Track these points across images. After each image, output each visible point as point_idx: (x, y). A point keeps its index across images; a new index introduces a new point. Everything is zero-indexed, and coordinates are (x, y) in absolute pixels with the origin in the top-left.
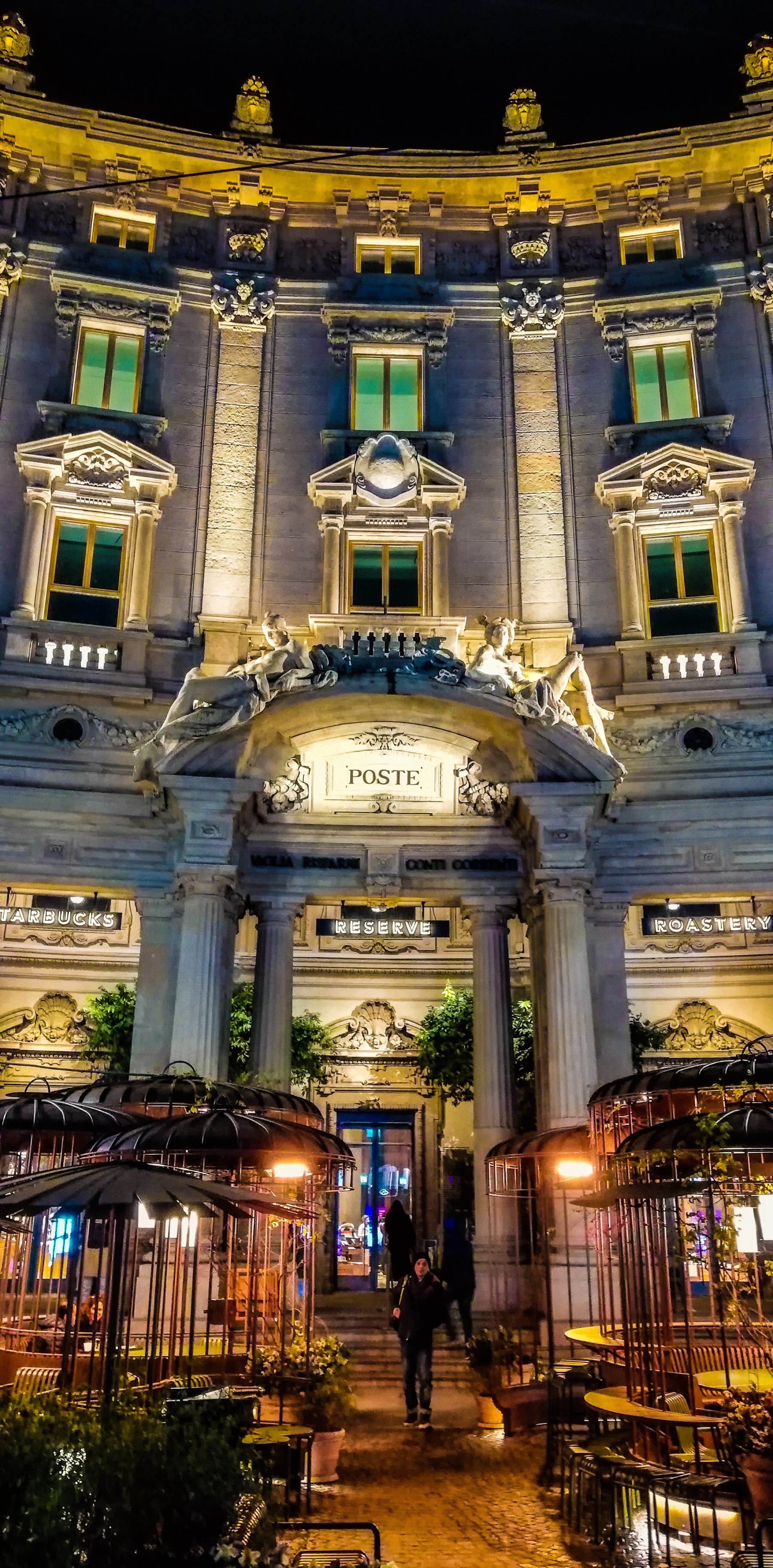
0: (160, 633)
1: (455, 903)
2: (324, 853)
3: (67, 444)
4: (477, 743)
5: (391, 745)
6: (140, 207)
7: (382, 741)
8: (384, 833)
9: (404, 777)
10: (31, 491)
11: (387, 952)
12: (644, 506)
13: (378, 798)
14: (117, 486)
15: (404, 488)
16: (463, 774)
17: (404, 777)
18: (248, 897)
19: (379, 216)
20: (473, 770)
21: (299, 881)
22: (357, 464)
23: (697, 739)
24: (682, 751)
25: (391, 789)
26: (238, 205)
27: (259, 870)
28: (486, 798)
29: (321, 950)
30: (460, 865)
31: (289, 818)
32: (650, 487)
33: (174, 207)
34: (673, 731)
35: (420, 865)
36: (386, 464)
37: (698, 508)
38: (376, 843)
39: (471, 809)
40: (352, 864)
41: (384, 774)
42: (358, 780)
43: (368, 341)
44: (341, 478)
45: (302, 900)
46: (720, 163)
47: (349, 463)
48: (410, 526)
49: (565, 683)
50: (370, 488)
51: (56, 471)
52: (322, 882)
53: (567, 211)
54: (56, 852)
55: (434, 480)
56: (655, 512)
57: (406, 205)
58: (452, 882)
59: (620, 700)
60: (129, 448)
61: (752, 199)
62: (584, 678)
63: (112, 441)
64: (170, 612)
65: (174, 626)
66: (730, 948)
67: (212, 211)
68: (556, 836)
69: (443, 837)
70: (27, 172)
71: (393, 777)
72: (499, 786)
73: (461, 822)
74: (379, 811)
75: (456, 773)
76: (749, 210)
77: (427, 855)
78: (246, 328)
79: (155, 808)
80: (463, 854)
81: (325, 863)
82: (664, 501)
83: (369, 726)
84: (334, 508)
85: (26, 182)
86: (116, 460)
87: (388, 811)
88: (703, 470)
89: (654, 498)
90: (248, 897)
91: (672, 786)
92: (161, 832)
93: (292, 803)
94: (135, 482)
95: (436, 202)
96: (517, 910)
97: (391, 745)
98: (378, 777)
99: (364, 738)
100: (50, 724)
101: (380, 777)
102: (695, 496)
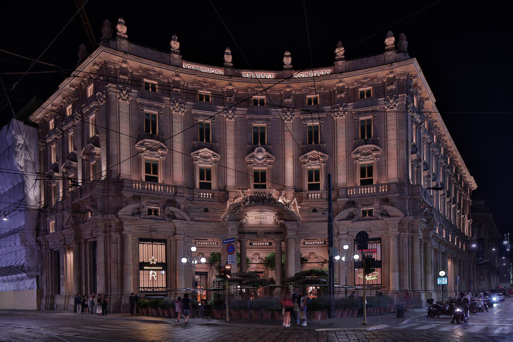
0: (220, 190)
1: (273, 239)
2: (251, 231)
6: (208, 90)
10: (194, 162)
13: (260, 222)
15: (263, 158)
21: (247, 236)
22: (254, 153)
25: (262, 220)
30: (273, 233)
31: (245, 226)
34: (310, 209)
36: (260, 153)
38: (259, 229)
40: (256, 233)
43: (255, 123)
47: (253, 153)
49: (293, 202)
50: (257, 158)
52: (251, 237)
53: (296, 90)
54: (207, 232)
55: (269, 157)
58: (272, 236)
59: (302, 203)
60: (211, 152)
61: (334, 91)
62: (296, 202)
64: (221, 185)
65: (222, 188)
67: (222, 90)
70: (184, 84)
73: (274, 226)
78: (231, 120)
83: (259, 209)
84: (251, 163)
86: (209, 154)
89: (310, 161)
91: (310, 219)
96: (283, 241)
101: (260, 218)
102: (318, 161)
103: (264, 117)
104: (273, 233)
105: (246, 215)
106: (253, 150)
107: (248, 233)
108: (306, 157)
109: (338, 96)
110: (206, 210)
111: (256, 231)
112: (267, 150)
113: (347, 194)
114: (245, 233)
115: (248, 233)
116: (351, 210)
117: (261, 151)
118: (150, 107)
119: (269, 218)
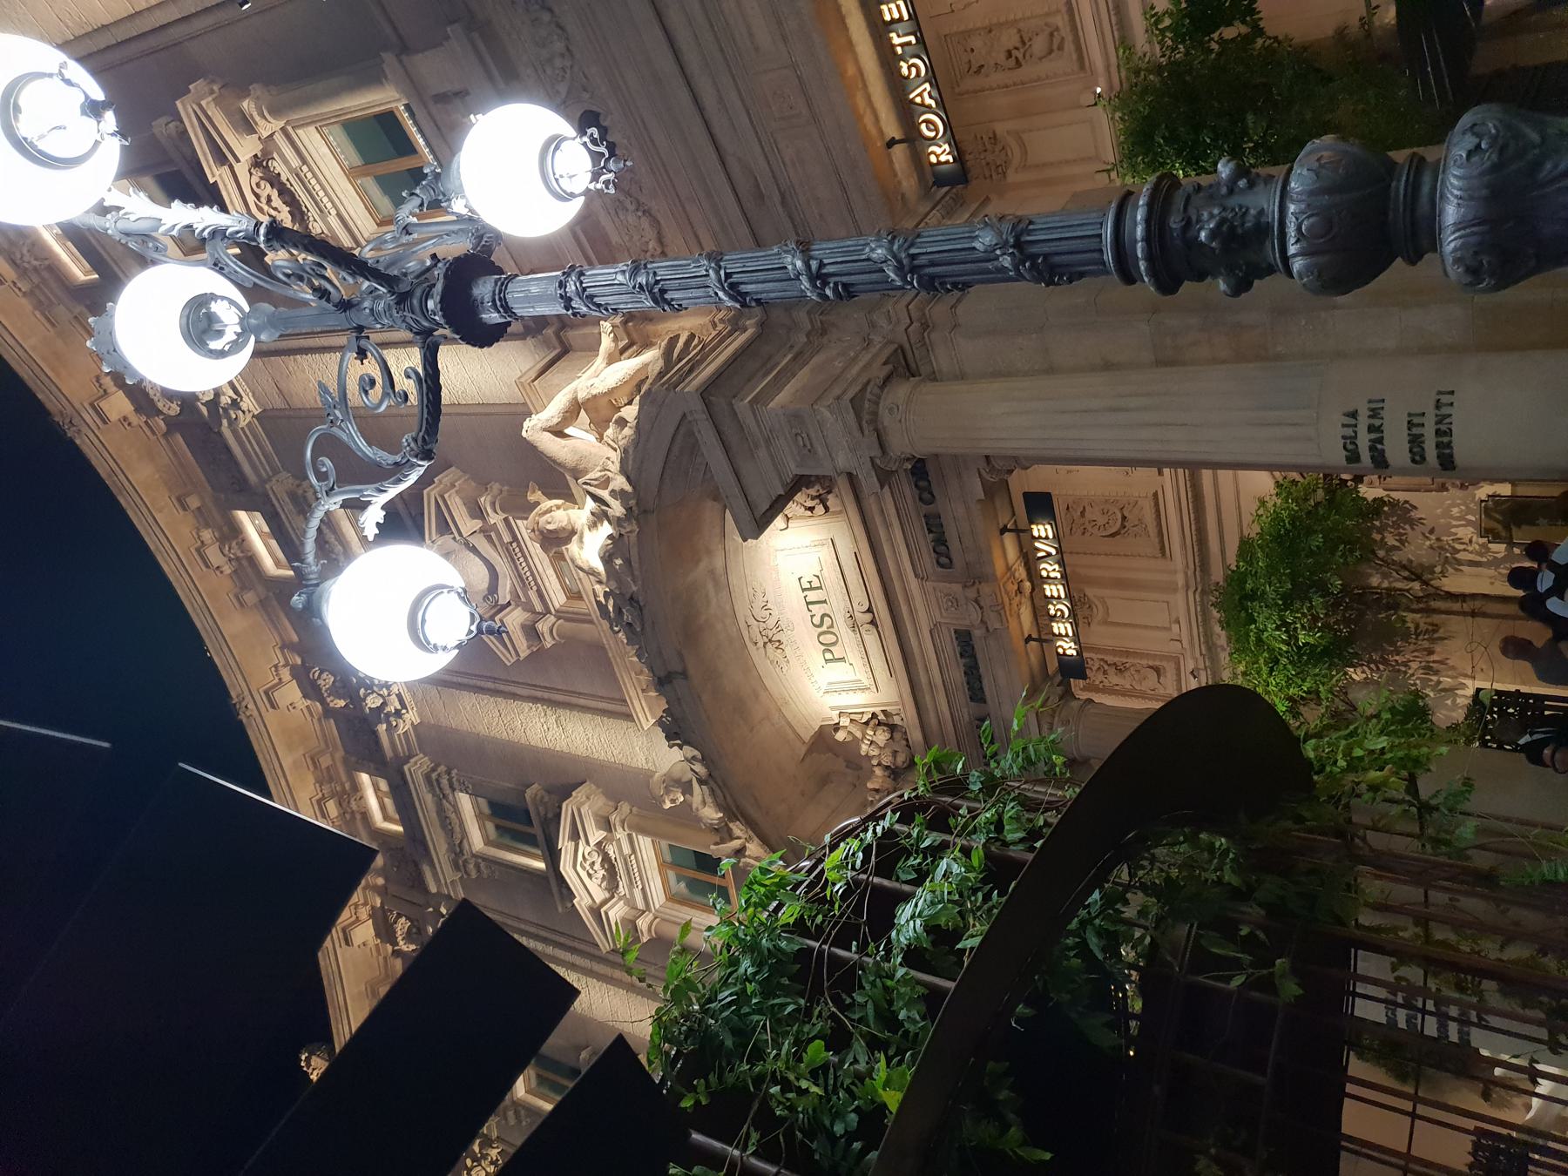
2: (957, 675)
3: (587, 901)
5: (771, 623)
8: (904, 609)
9: (812, 596)
14: (611, 850)
17: (812, 596)
25: (838, 606)
33: (340, 754)
37: (295, 162)
40: (964, 640)
41: (817, 620)
48: (515, 538)
51: (616, 912)
56: (333, 221)
57: (207, 535)
69: (888, 526)
74: (873, 622)
77: (924, 542)
81: (973, 674)
82: (313, 213)
85: (385, 887)
87: (870, 610)
88: (242, 170)
94: (596, 835)
97: (771, 623)
98: (824, 628)
101: (823, 625)
111: (950, 647)
119: (797, 563)
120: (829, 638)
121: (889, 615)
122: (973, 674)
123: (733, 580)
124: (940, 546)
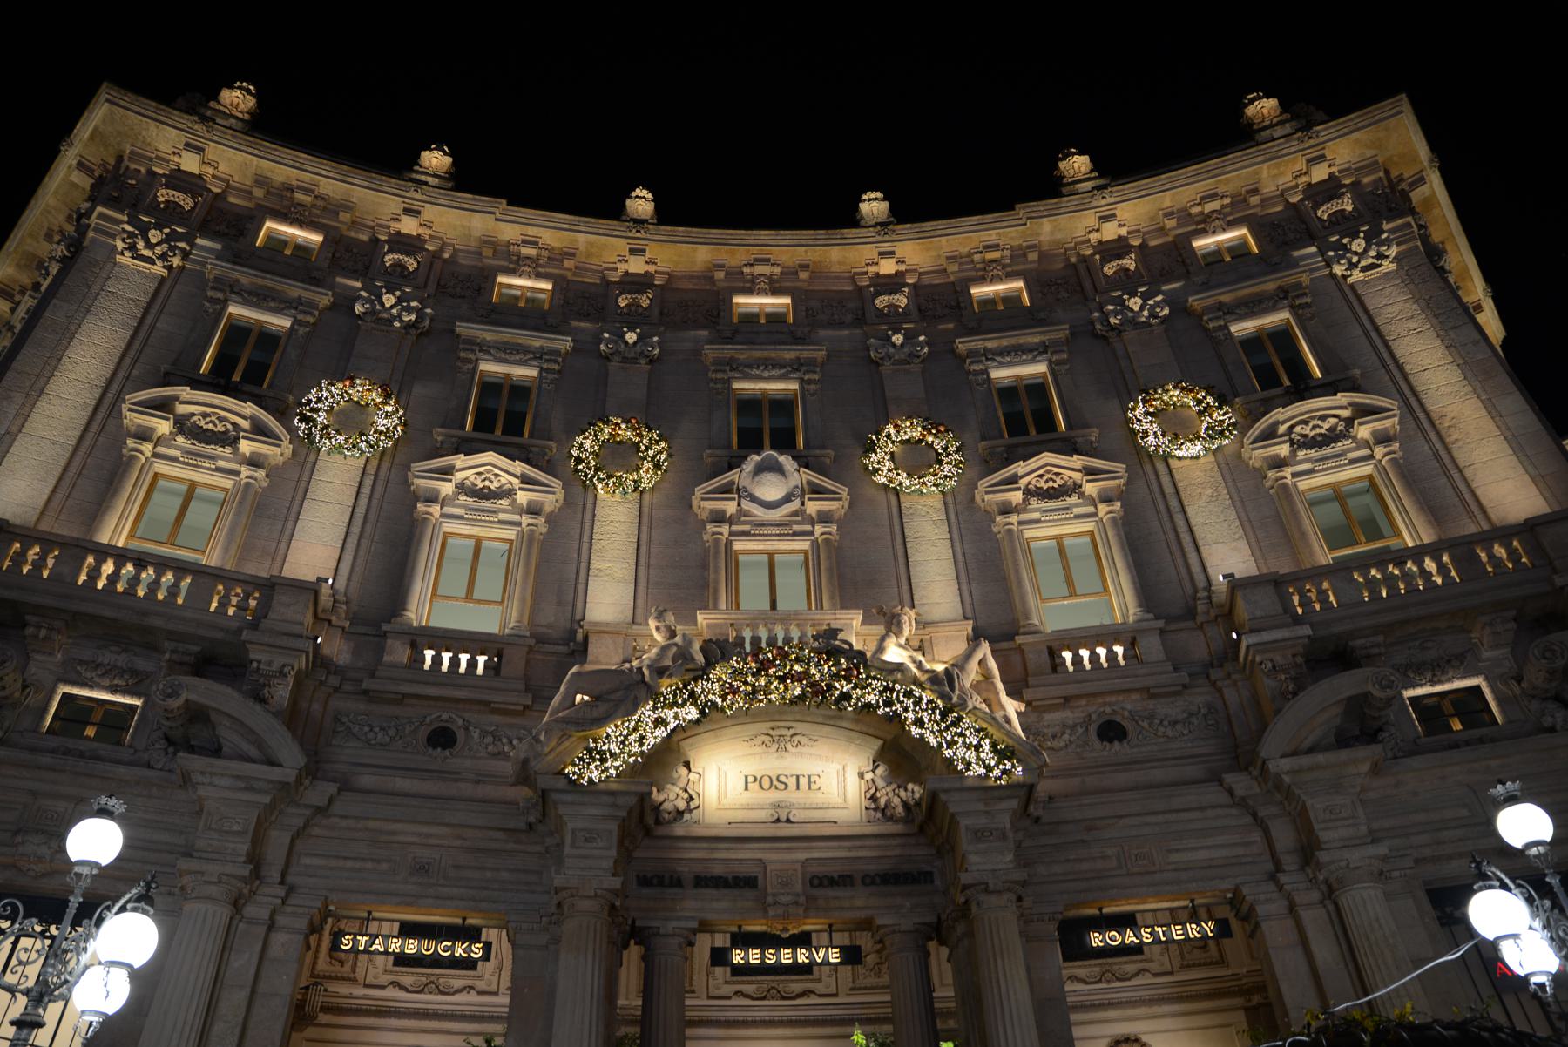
0: (541, 639)
1: (866, 925)
2: (718, 870)
3: (459, 465)
4: (880, 742)
5: (789, 746)
7: (777, 742)
8: (784, 845)
10: (421, 506)
11: (784, 998)
12: (1025, 511)
13: (778, 806)
14: (504, 503)
15: (787, 499)
16: (869, 776)
17: (804, 781)
18: (634, 921)
19: (754, 278)
20: (880, 771)
21: (692, 905)
22: (740, 477)
23: (1111, 731)
24: (1097, 744)
25: (791, 796)
26: (627, 273)
27: (646, 891)
28: (896, 801)
29: (710, 998)
30: (869, 880)
31: (679, 830)
32: (1028, 493)
33: (569, 275)
34: (1087, 721)
35: (826, 882)
36: (769, 478)
37: (1077, 511)
38: (775, 858)
39: (879, 815)
40: (749, 882)
41: (783, 779)
42: (753, 786)
43: (748, 378)
44: (727, 489)
45: (695, 924)
46: (1052, 233)
47: (733, 475)
48: (795, 534)
50: (754, 499)
51: (447, 488)
52: (718, 905)
55: (816, 490)
56: (1036, 515)
57: (777, 270)
58: (860, 902)
59: (1027, 694)
61: (1084, 259)
63: (503, 462)
66: (1156, 975)
67: (603, 278)
68: (978, 835)
69: (850, 849)
70: (441, 250)
71: (792, 782)
72: (910, 786)
74: (778, 820)
75: (861, 776)
76: (1082, 269)
77: (834, 870)
79: (532, 819)
80: (872, 868)
81: (720, 882)
82: (1043, 505)
84: (719, 518)
85: (440, 258)
86: (505, 478)
87: (788, 821)
88: (1077, 476)
89: (1034, 502)
90: (634, 921)
92: (538, 848)
93: (680, 813)
94: (522, 497)
95: (804, 267)
96: (937, 931)
97: (789, 746)
99: (758, 741)
100: (424, 732)
101: (777, 782)
102: (1074, 499)
103: (789, 354)
104: (869, 880)
105: (687, 765)
106: (734, 463)
107: (702, 881)
108: (1014, 480)
109: (1109, 270)
110: (442, 738)
111: (753, 870)
112: (804, 462)
113: (1288, 608)
114: (677, 882)
115: (702, 881)
116: (1347, 684)
117: (779, 469)
118: (258, 298)
119: (835, 780)
120: (766, 784)
121: (782, 834)
122: (720, 882)
123: (827, 729)
124: (833, 882)
